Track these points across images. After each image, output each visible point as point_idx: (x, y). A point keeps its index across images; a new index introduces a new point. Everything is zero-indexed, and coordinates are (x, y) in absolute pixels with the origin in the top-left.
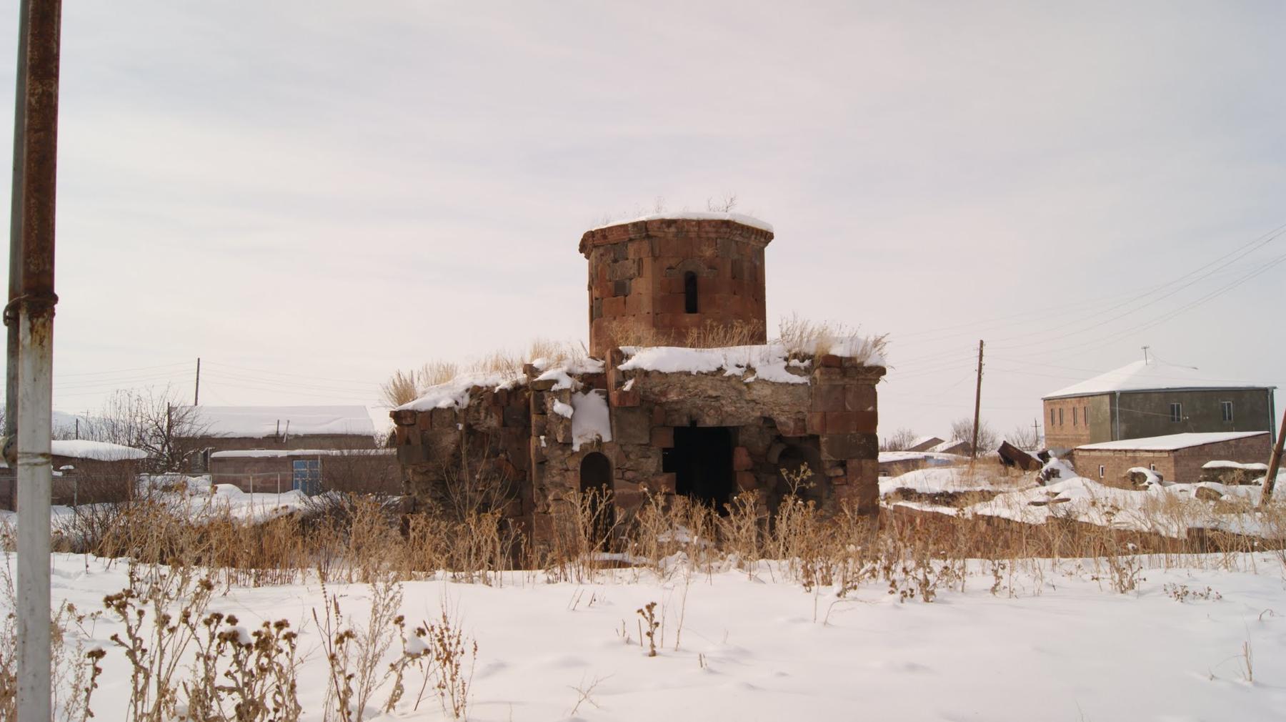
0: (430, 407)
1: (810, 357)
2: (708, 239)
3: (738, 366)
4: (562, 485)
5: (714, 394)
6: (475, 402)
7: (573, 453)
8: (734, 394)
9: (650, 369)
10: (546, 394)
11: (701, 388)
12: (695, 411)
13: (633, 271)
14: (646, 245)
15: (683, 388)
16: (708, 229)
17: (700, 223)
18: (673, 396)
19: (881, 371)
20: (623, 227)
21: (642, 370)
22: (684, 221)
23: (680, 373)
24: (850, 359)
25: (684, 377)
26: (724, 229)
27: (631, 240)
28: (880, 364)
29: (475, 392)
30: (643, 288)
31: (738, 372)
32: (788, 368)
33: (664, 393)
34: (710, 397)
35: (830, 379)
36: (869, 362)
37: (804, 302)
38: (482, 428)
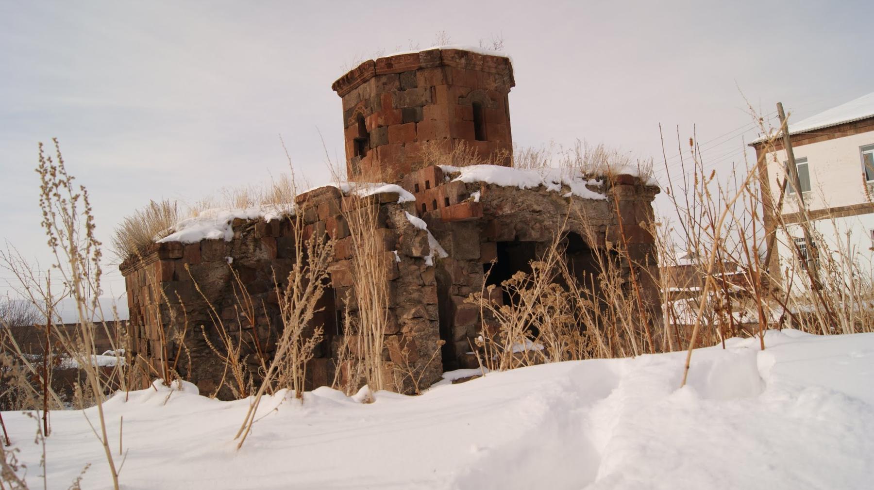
0: (198, 239)
1: (604, 178)
2: (489, 74)
3: (554, 183)
4: (420, 302)
5: (536, 207)
6: (239, 234)
7: (429, 268)
8: (551, 208)
9: (490, 183)
10: (391, 208)
11: (529, 202)
12: (519, 225)
13: (426, 96)
14: (438, 73)
15: (514, 203)
16: (490, 64)
17: (485, 58)
18: (507, 210)
19: (656, 190)
20: (417, 55)
21: (485, 183)
22: (473, 54)
23: (513, 187)
24: (638, 179)
25: (514, 192)
26: (502, 66)
27: (421, 69)
28: (656, 184)
29: (237, 224)
30: (438, 113)
31: (557, 188)
32: (587, 186)
33: (500, 207)
34: (534, 211)
35: (626, 195)
36: (649, 183)
37: (552, 138)
38: (251, 262)
